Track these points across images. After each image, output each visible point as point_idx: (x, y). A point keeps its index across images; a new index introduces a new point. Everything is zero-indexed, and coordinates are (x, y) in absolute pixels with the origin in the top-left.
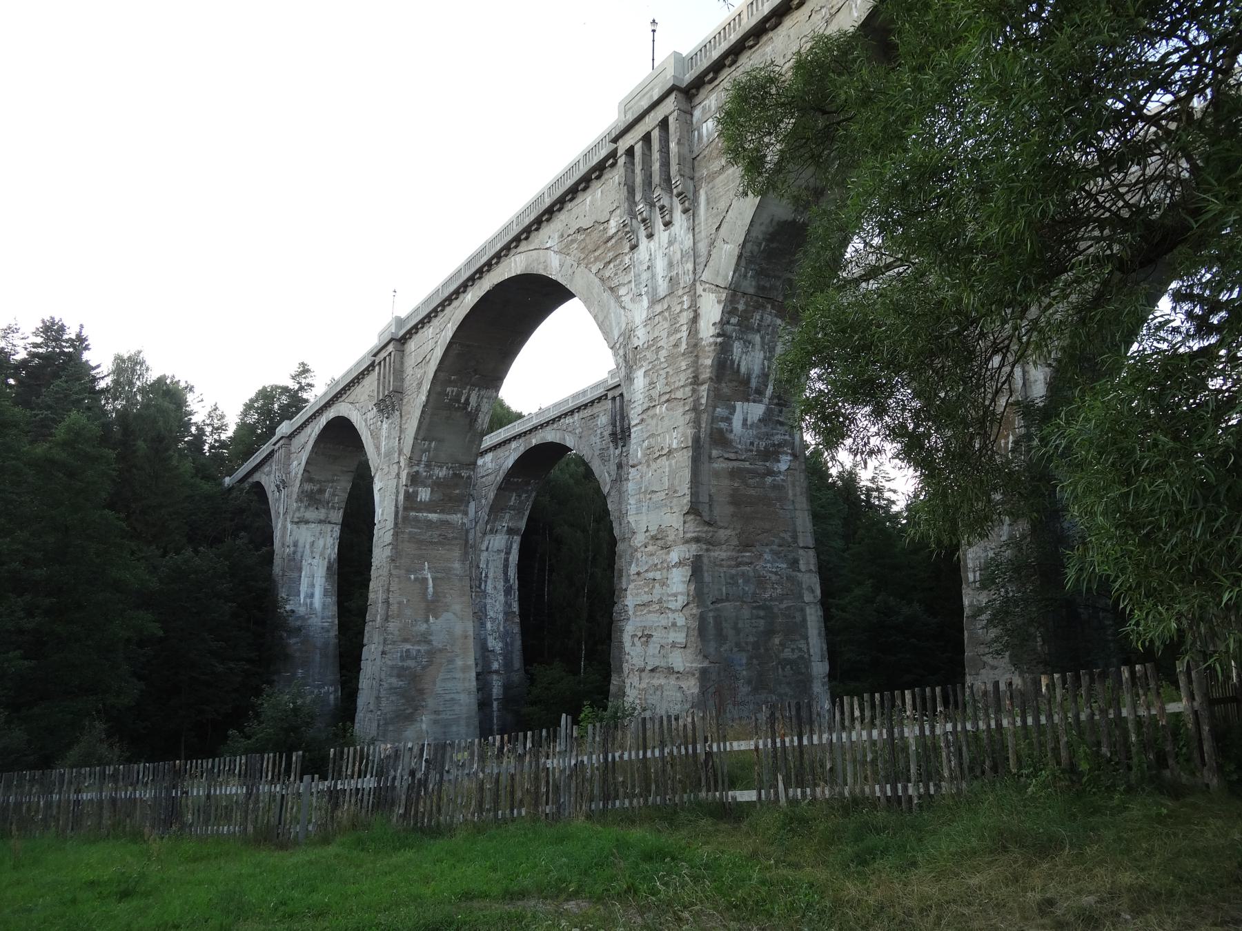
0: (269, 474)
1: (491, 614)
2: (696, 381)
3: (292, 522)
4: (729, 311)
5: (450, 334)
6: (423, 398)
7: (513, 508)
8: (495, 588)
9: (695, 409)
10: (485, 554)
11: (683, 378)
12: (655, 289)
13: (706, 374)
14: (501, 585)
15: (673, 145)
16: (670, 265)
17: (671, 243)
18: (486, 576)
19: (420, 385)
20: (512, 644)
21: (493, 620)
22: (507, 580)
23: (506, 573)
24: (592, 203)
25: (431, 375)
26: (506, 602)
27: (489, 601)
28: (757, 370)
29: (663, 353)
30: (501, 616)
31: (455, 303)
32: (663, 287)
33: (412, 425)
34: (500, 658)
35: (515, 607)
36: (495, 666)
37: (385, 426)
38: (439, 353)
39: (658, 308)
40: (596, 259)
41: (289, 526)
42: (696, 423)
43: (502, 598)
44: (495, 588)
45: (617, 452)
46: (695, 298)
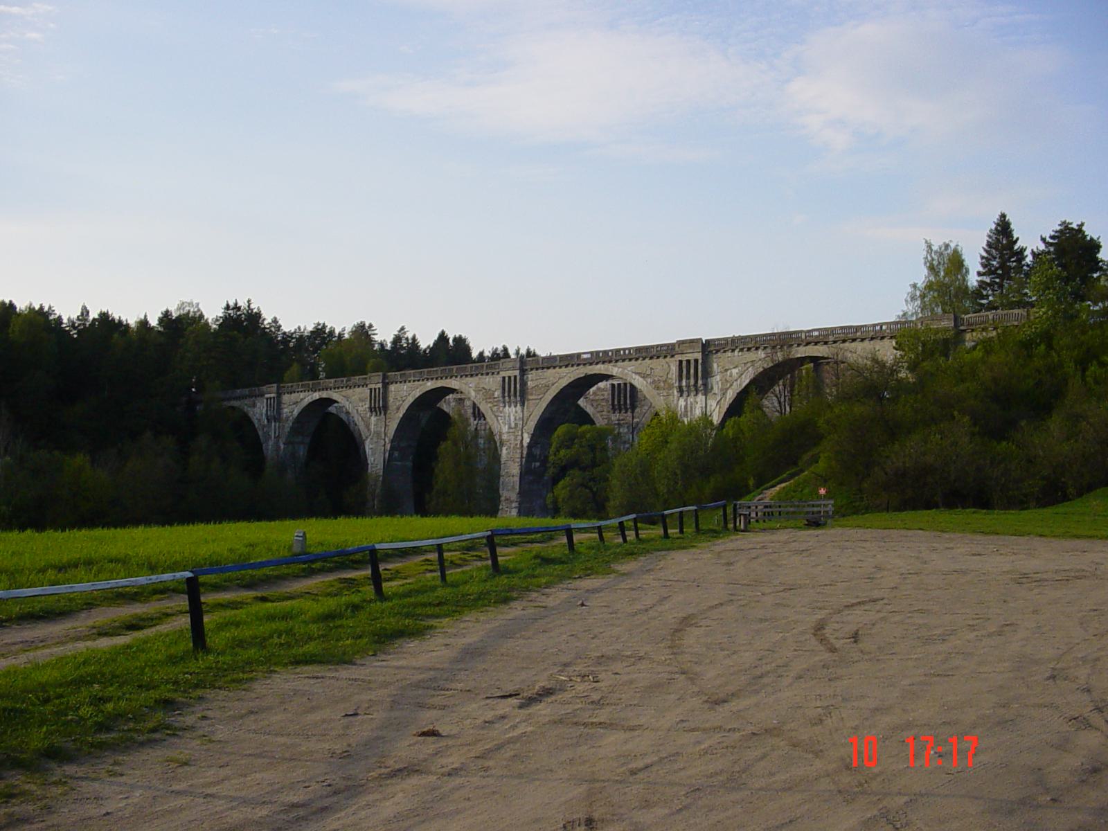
0: (254, 406)
2: (522, 457)
3: (284, 444)
4: (531, 439)
5: (418, 395)
6: (401, 416)
9: (521, 465)
11: (518, 456)
12: (510, 424)
13: (524, 456)
15: (518, 386)
16: (515, 419)
17: (516, 412)
19: (398, 409)
24: (489, 382)
25: (406, 407)
28: (538, 453)
29: (512, 446)
31: (421, 382)
32: (513, 425)
33: (393, 425)
37: (373, 419)
38: (411, 400)
39: (511, 430)
40: (490, 402)
41: (282, 446)
42: (521, 469)
45: (476, 422)
46: (522, 433)
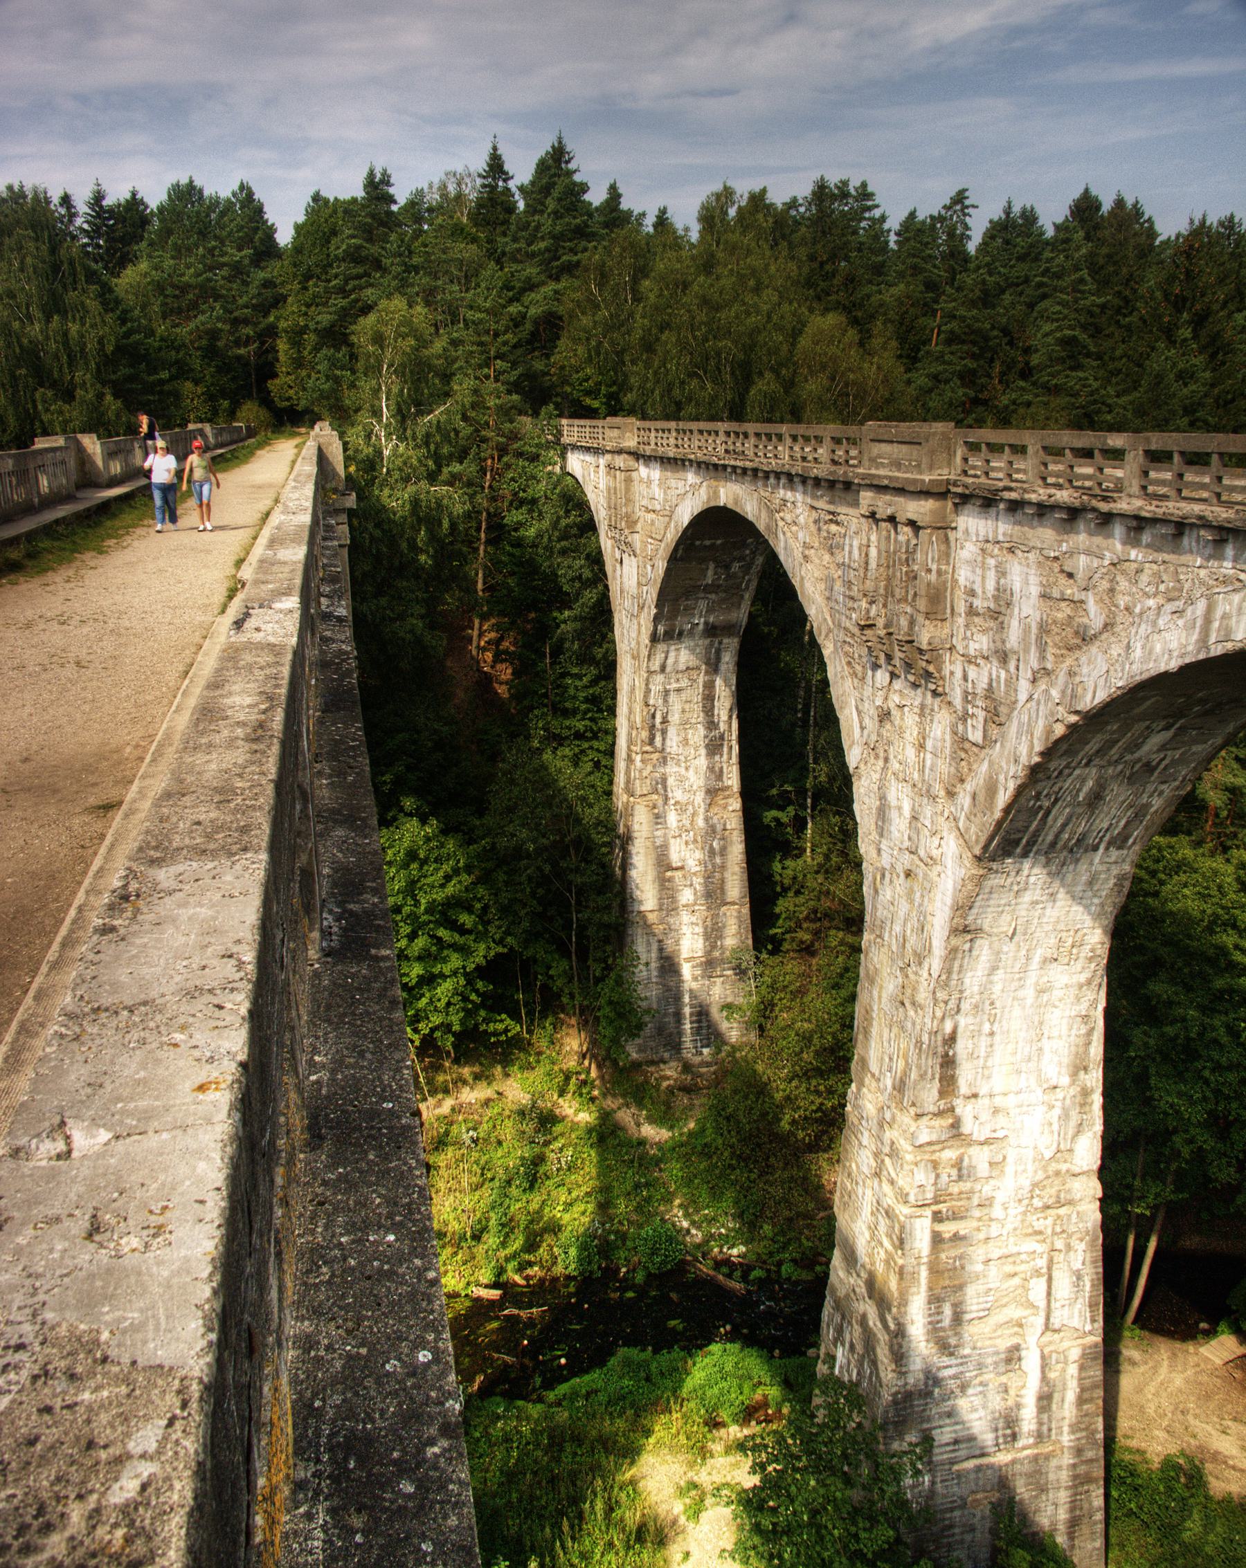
1: (677, 794)
7: (708, 589)
8: (685, 742)
10: (659, 678)
14: (698, 735)
18: (665, 721)
20: (723, 851)
21: (681, 808)
22: (711, 725)
23: (709, 710)
26: (711, 769)
27: (671, 769)
30: (699, 798)
34: (698, 881)
35: (733, 779)
36: (686, 896)
43: (702, 762)
44: (685, 742)
